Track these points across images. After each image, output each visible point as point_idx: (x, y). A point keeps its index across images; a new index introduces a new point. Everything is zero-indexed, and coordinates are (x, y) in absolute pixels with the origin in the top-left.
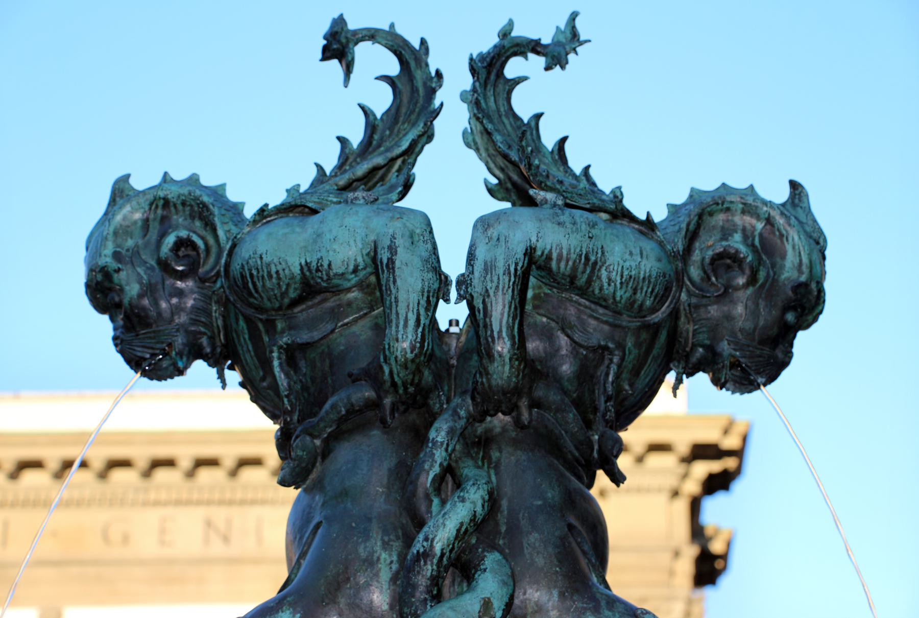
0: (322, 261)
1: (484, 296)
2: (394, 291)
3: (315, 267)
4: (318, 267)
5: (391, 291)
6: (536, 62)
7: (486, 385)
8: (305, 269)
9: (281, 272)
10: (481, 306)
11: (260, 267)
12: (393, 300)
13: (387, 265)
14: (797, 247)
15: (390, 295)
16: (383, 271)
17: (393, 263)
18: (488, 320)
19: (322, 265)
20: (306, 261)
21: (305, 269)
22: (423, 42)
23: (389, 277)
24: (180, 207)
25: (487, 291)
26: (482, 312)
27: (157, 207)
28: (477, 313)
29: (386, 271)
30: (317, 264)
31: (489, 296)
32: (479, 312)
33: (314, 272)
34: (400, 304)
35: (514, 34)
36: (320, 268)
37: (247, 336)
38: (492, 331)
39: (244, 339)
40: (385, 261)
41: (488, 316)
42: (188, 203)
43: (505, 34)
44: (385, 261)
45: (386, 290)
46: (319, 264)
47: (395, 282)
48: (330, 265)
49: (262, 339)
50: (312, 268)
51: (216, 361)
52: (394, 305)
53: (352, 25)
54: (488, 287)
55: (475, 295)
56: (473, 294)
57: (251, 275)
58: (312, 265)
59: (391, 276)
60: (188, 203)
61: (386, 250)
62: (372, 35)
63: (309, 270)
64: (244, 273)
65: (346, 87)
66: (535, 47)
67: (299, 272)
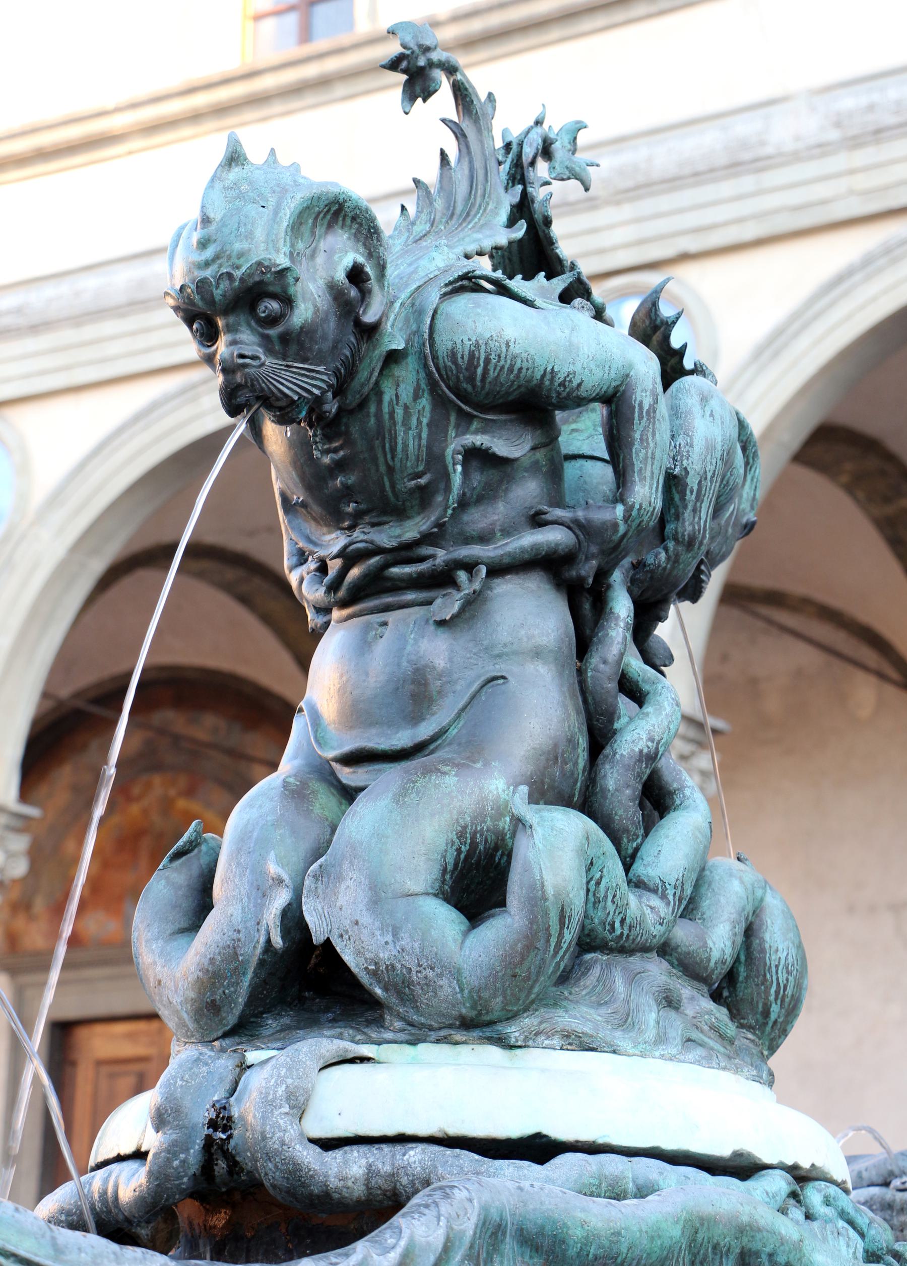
0: (574, 377)
1: (701, 477)
2: (652, 445)
3: (561, 380)
4: (565, 380)
5: (648, 444)
7: (667, 571)
8: (548, 376)
9: (524, 371)
10: (695, 488)
11: (503, 356)
12: (650, 455)
13: (648, 412)
14: (755, 480)
15: (646, 448)
16: (641, 417)
17: (655, 412)
18: (698, 504)
19: (570, 381)
20: (553, 369)
21: (548, 376)
22: (490, 95)
23: (648, 427)
24: (348, 221)
25: (706, 472)
26: (695, 493)
27: (329, 209)
28: (688, 492)
29: (645, 419)
30: (565, 378)
31: (706, 479)
32: (692, 492)
33: (556, 384)
34: (656, 462)
36: (567, 383)
37: (425, 421)
38: (700, 518)
39: (419, 422)
40: (646, 407)
41: (700, 500)
42: (359, 220)
44: (646, 407)
45: (641, 439)
46: (568, 379)
47: (654, 435)
48: (579, 385)
49: (448, 431)
50: (556, 379)
52: (649, 460)
54: (707, 469)
55: (692, 473)
56: (688, 469)
57: (487, 361)
58: (559, 376)
59: (651, 426)
60: (359, 220)
61: (648, 393)
63: (552, 380)
64: (477, 354)
65: (407, 113)
67: (539, 377)
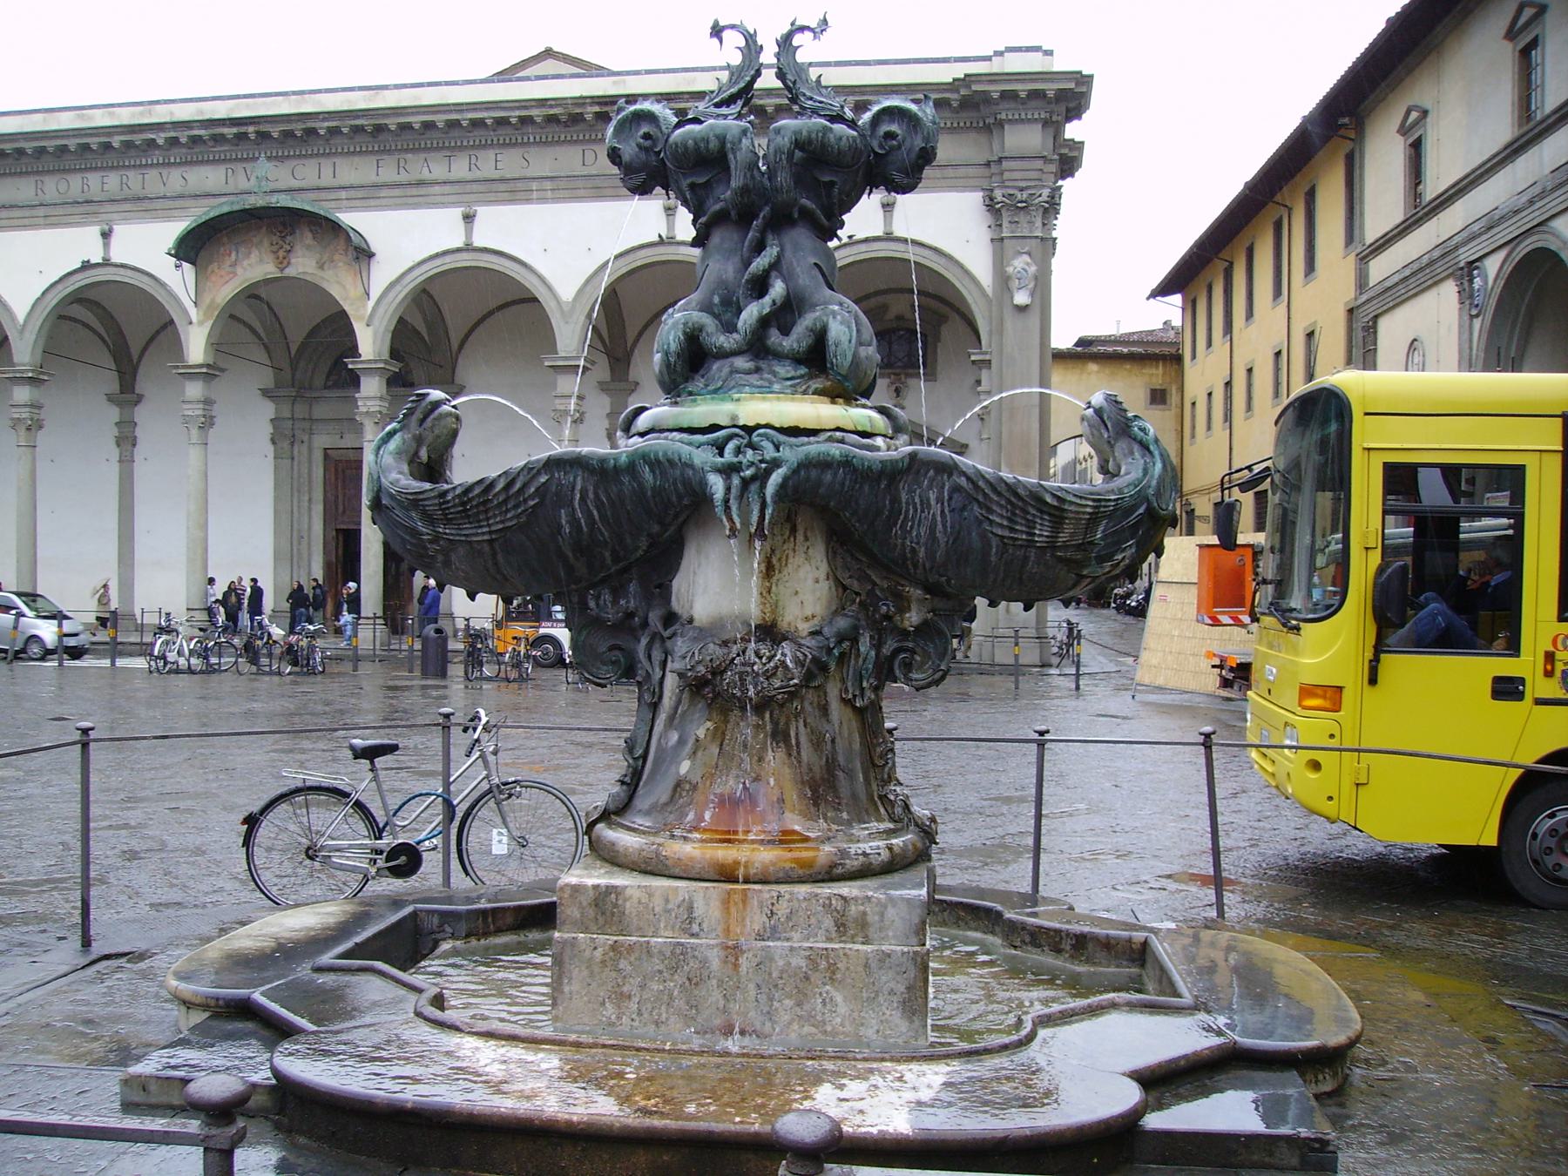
6: (808, 35)
35: (798, 23)
43: (792, 24)
51: (666, 187)
53: (721, 24)
62: (733, 27)
66: (808, 28)
